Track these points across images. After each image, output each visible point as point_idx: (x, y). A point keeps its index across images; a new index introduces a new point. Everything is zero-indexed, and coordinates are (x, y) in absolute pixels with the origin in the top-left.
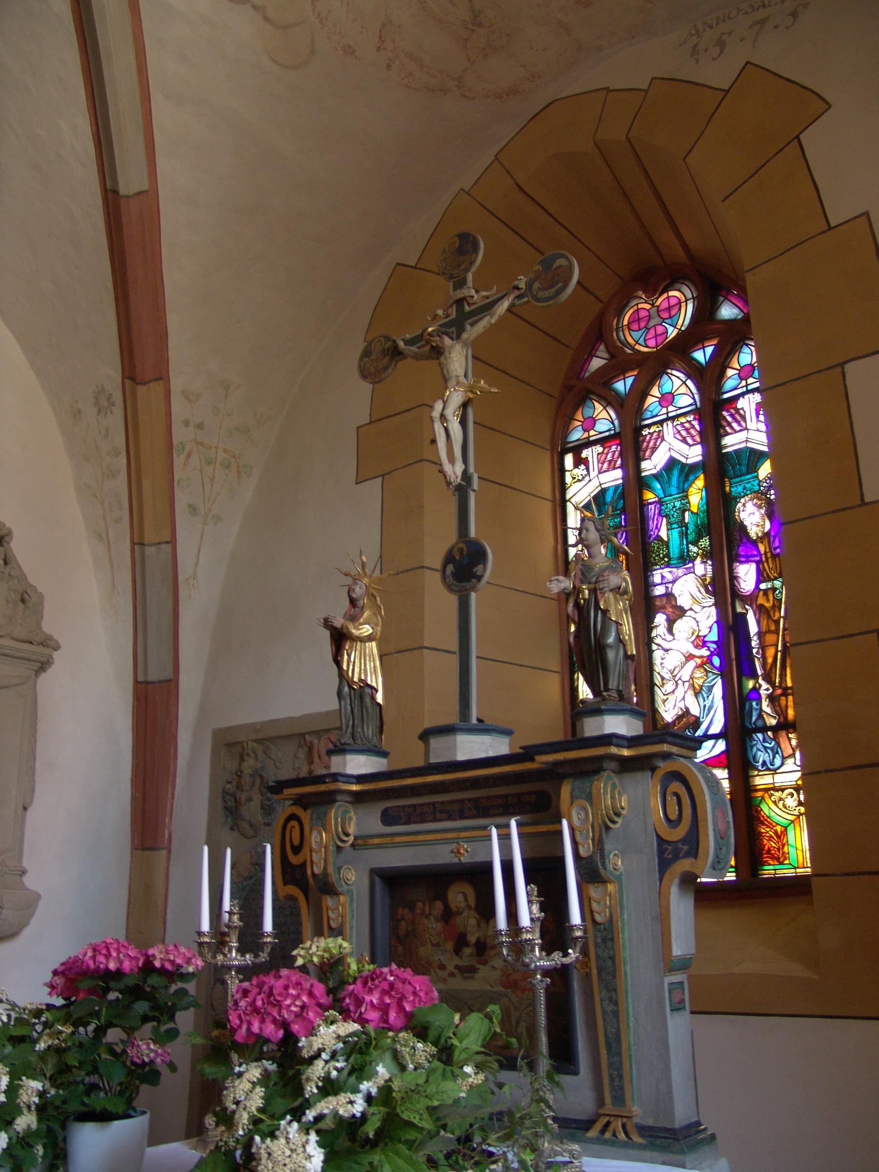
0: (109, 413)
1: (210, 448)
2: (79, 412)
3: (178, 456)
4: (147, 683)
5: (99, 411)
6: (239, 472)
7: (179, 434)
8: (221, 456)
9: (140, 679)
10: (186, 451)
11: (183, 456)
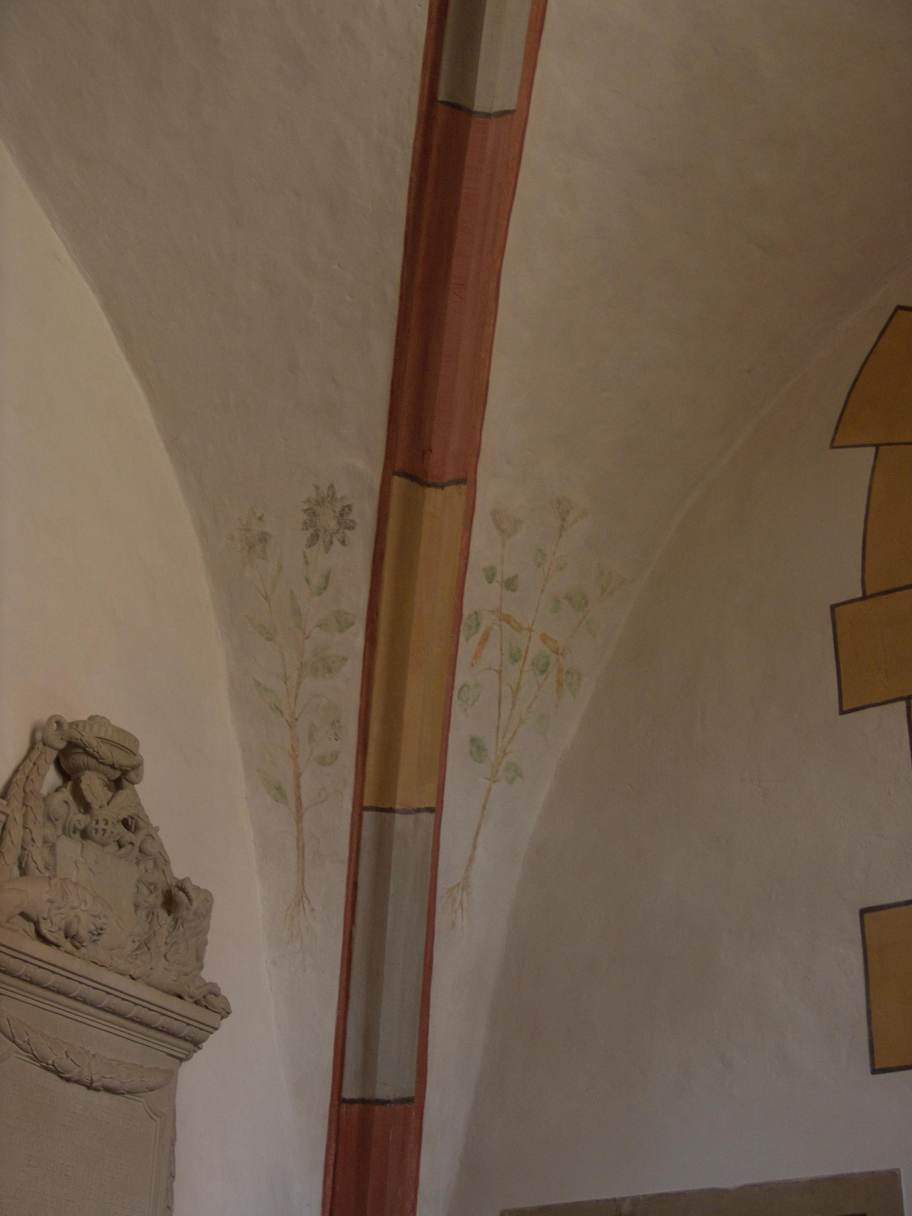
0: (337, 544)
1: (520, 629)
2: (264, 538)
3: (467, 640)
4: (367, 1103)
5: (314, 539)
6: (559, 683)
7: (479, 596)
8: (536, 647)
9: (349, 1092)
10: (482, 629)
11: (476, 639)
